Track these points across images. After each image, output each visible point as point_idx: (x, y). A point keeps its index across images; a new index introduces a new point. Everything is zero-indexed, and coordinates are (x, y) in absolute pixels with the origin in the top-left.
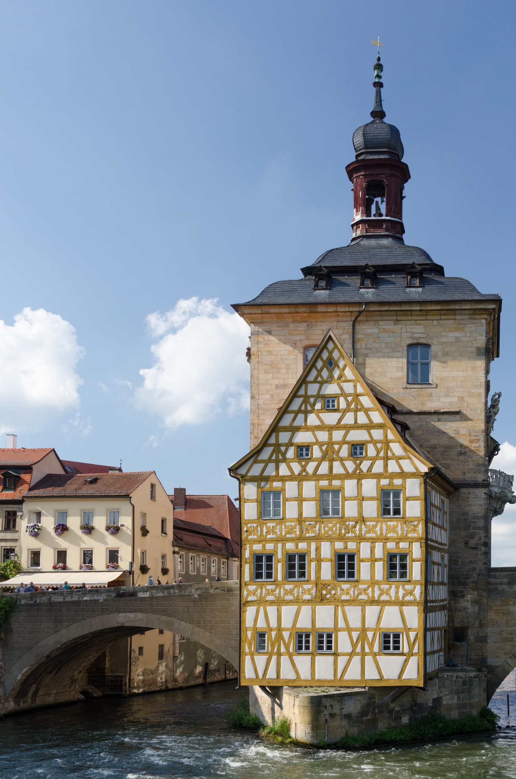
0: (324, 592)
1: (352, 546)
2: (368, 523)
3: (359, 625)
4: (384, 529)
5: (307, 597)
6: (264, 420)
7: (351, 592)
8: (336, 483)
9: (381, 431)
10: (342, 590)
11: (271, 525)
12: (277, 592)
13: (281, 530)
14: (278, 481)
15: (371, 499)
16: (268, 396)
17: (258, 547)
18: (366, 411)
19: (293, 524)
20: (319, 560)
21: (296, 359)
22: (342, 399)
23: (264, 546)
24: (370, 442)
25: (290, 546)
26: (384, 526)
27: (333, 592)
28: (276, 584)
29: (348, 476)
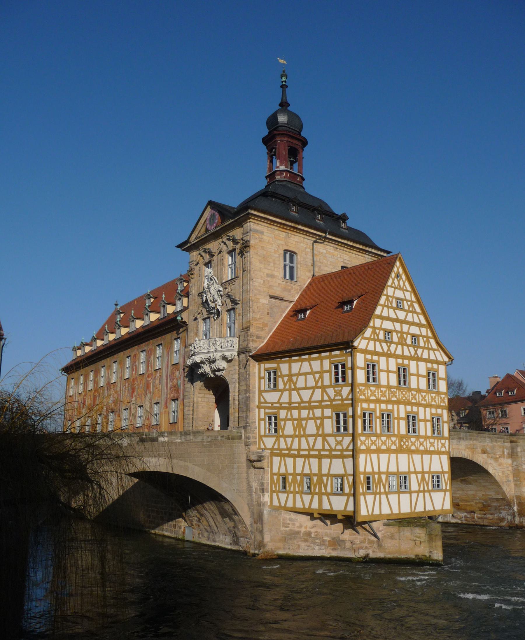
0: (402, 443)
1: (415, 409)
2: (422, 394)
3: (421, 470)
4: (430, 399)
5: (394, 447)
8: (406, 362)
9: (425, 329)
10: (411, 442)
11: (373, 389)
12: (377, 443)
14: (376, 355)
15: (423, 376)
16: (262, 281)
17: (365, 405)
19: (385, 389)
22: (405, 302)
23: (369, 406)
25: (383, 406)
27: (407, 443)
29: (410, 358)
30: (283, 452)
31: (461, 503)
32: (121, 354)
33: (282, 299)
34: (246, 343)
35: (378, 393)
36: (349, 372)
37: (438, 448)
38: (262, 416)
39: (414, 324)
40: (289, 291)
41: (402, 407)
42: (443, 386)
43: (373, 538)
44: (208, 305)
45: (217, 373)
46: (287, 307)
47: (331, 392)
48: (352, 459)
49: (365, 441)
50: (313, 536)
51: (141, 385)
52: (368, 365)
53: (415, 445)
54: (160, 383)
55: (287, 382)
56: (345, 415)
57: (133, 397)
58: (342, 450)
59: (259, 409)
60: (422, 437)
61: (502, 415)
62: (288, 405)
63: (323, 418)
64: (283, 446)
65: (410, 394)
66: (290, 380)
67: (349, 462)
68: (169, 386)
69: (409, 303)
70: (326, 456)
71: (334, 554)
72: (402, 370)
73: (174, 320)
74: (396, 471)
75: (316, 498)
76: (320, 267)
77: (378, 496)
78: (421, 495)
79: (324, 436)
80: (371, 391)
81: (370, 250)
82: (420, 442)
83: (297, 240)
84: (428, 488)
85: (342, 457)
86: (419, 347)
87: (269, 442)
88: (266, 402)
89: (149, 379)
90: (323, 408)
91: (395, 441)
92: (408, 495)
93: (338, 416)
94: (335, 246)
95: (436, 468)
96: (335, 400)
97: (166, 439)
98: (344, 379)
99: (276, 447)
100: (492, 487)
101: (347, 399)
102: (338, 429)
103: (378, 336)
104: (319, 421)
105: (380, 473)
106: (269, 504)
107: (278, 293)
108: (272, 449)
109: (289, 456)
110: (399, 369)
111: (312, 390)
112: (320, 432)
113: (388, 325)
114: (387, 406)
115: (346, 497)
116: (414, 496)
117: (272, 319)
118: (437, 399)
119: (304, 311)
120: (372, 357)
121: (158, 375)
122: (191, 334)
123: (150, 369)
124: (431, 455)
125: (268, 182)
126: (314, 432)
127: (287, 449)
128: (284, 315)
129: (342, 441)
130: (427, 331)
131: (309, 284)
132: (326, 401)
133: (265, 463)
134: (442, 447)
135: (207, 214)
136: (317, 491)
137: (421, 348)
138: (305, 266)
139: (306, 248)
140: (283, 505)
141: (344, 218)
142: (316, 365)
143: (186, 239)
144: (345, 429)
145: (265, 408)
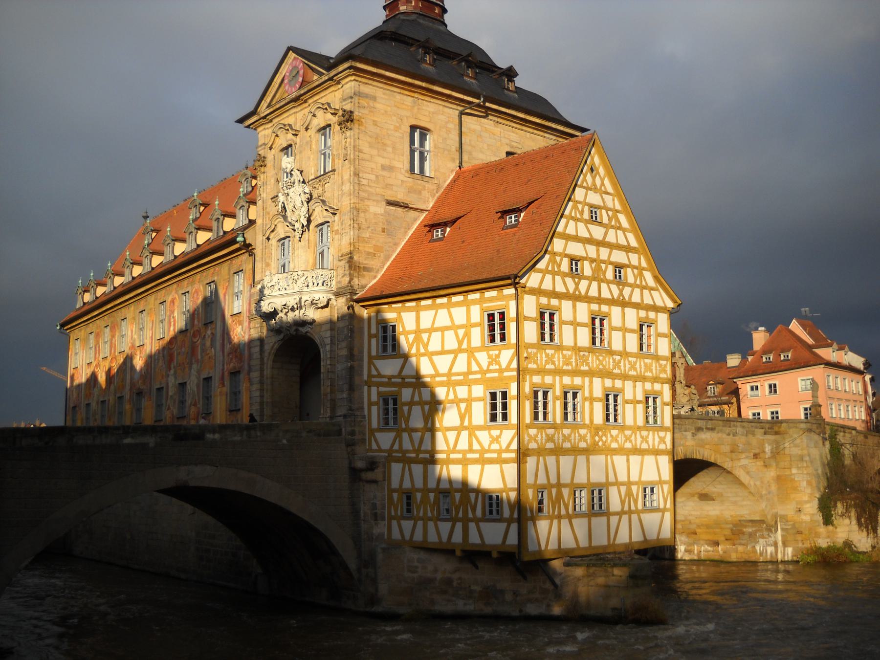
0: (597, 438)
1: (618, 384)
2: (630, 359)
6: (368, 206)
7: (619, 439)
8: (605, 308)
9: (636, 256)
10: (612, 436)
13: (559, 360)
15: (632, 331)
16: (373, 177)
17: (537, 379)
18: (624, 230)
19: (570, 353)
20: (592, 400)
21: (403, 138)
22: (604, 211)
23: (543, 379)
24: (628, 266)
25: (567, 380)
26: (643, 364)
27: (604, 439)
28: (555, 428)
29: (612, 302)
30: (408, 455)
31: (698, 531)
32: (151, 299)
33: (406, 207)
34: (348, 279)
35: (559, 358)
36: (511, 328)
37: (654, 444)
38: (374, 398)
39: (619, 247)
40: (420, 193)
41: (597, 381)
42: (664, 347)
43: (548, 585)
44: (285, 217)
45: (301, 329)
46: (415, 220)
47: (483, 358)
48: (516, 465)
49: (536, 436)
50: (455, 584)
51: (183, 350)
52: (542, 314)
53: (617, 441)
54: (213, 345)
55: (413, 343)
56: (504, 395)
57: (170, 369)
58: (500, 452)
59: (369, 387)
60: (629, 428)
61: (771, 392)
62: (414, 380)
63: (469, 401)
64: (407, 445)
65: (611, 361)
66: (418, 339)
67: (511, 470)
68: (226, 350)
69: (610, 213)
70: (475, 461)
71: (488, 610)
72: (597, 322)
73: (233, 241)
74: (585, 481)
75: (459, 526)
76: (470, 153)
77: (555, 522)
78: (625, 518)
79: (472, 430)
80: (547, 355)
81: (554, 126)
82: (625, 436)
83: (432, 110)
84: (636, 505)
85: (502, 461)
86: (626, 284)
87: (385, 440)
88: (380, 375)
89: (195, 340)
90: (469, 383)
91: (585, 435)
92: (604, 519)
93: (493, 396)
94: (495, 119)
95: (650, 475)
96: (489, 371)
97: (217, 436)
98: (503, 338)
99: (396, 447)
100: (745, 503)
101: (508, 369)
102: (493, 418)
103: (559, 266)
104: (463, 406)
105: (559, 485)
106: (386, 537)
107: (400, 197)
108: (390, 451)
109: (416, 461)
110: (593, 320)
111: (452, 356)
112: (466, 423)
113: (576, 249)
114: (572, 381)
115: (505, 524)
116: (614, 520)
117: (390, 240)
118: (654, 368)
119: (443, 225)
120: (549, 301)
121: (209, 332)
122: (258, 265)
123: (196, 322)
124: (643, 455)
125: (387, 16)
126: (457, 422)
127: (414, 451)
128: (411, 232)
129: (499, 436)
130: (640, 259)
131: (454, 181)
132: (476, 373)
133: (377, 474)
134: (659, 443)
135: (285, 70)
136: (460, 515)
137: (630, 285)
138: (446, 152)
139: (446, 123)
140: (407, 537)
141: (510, 74)
142: (459, 315)
143: (252, 109)
144: (505, 417)
145: (378, 385)
